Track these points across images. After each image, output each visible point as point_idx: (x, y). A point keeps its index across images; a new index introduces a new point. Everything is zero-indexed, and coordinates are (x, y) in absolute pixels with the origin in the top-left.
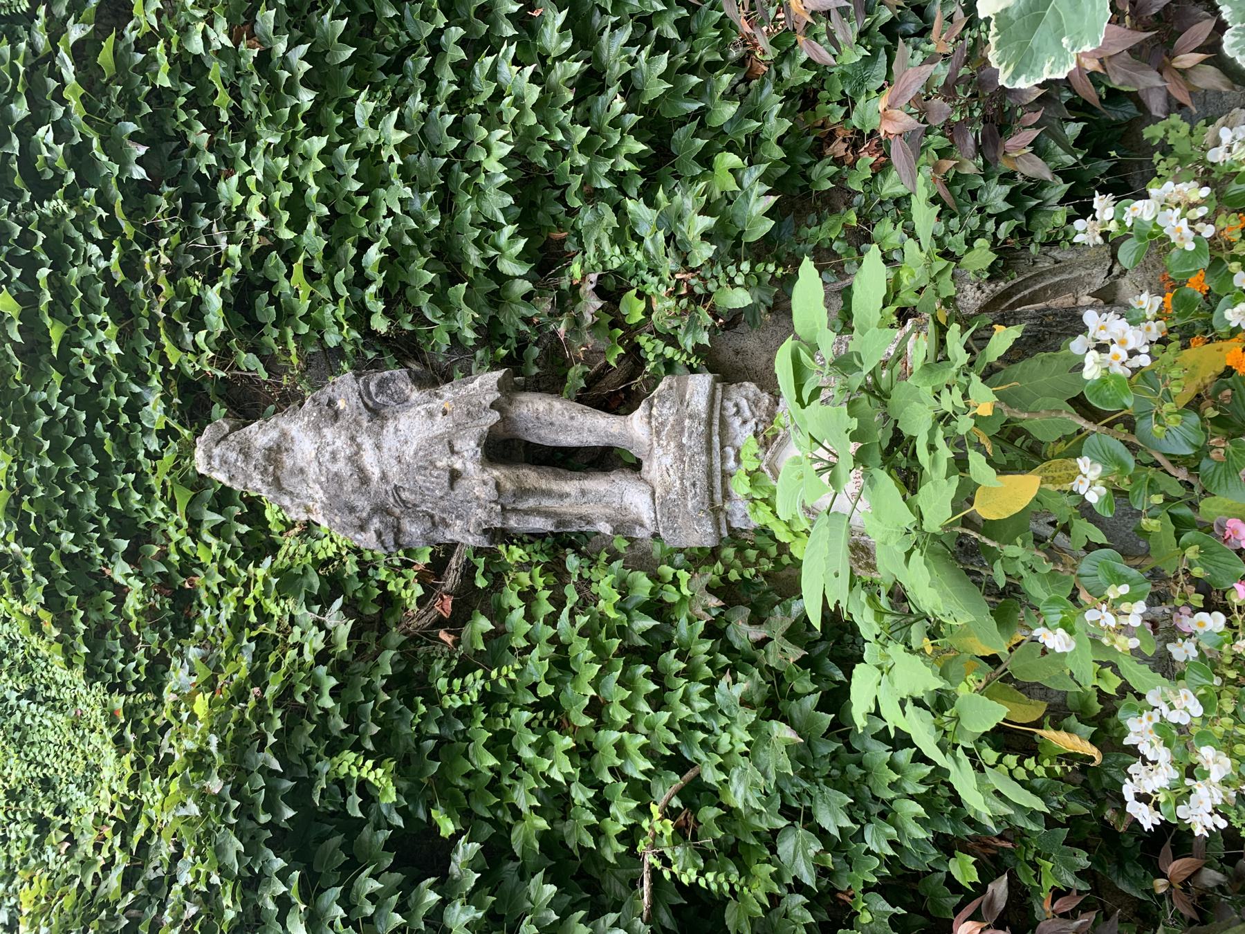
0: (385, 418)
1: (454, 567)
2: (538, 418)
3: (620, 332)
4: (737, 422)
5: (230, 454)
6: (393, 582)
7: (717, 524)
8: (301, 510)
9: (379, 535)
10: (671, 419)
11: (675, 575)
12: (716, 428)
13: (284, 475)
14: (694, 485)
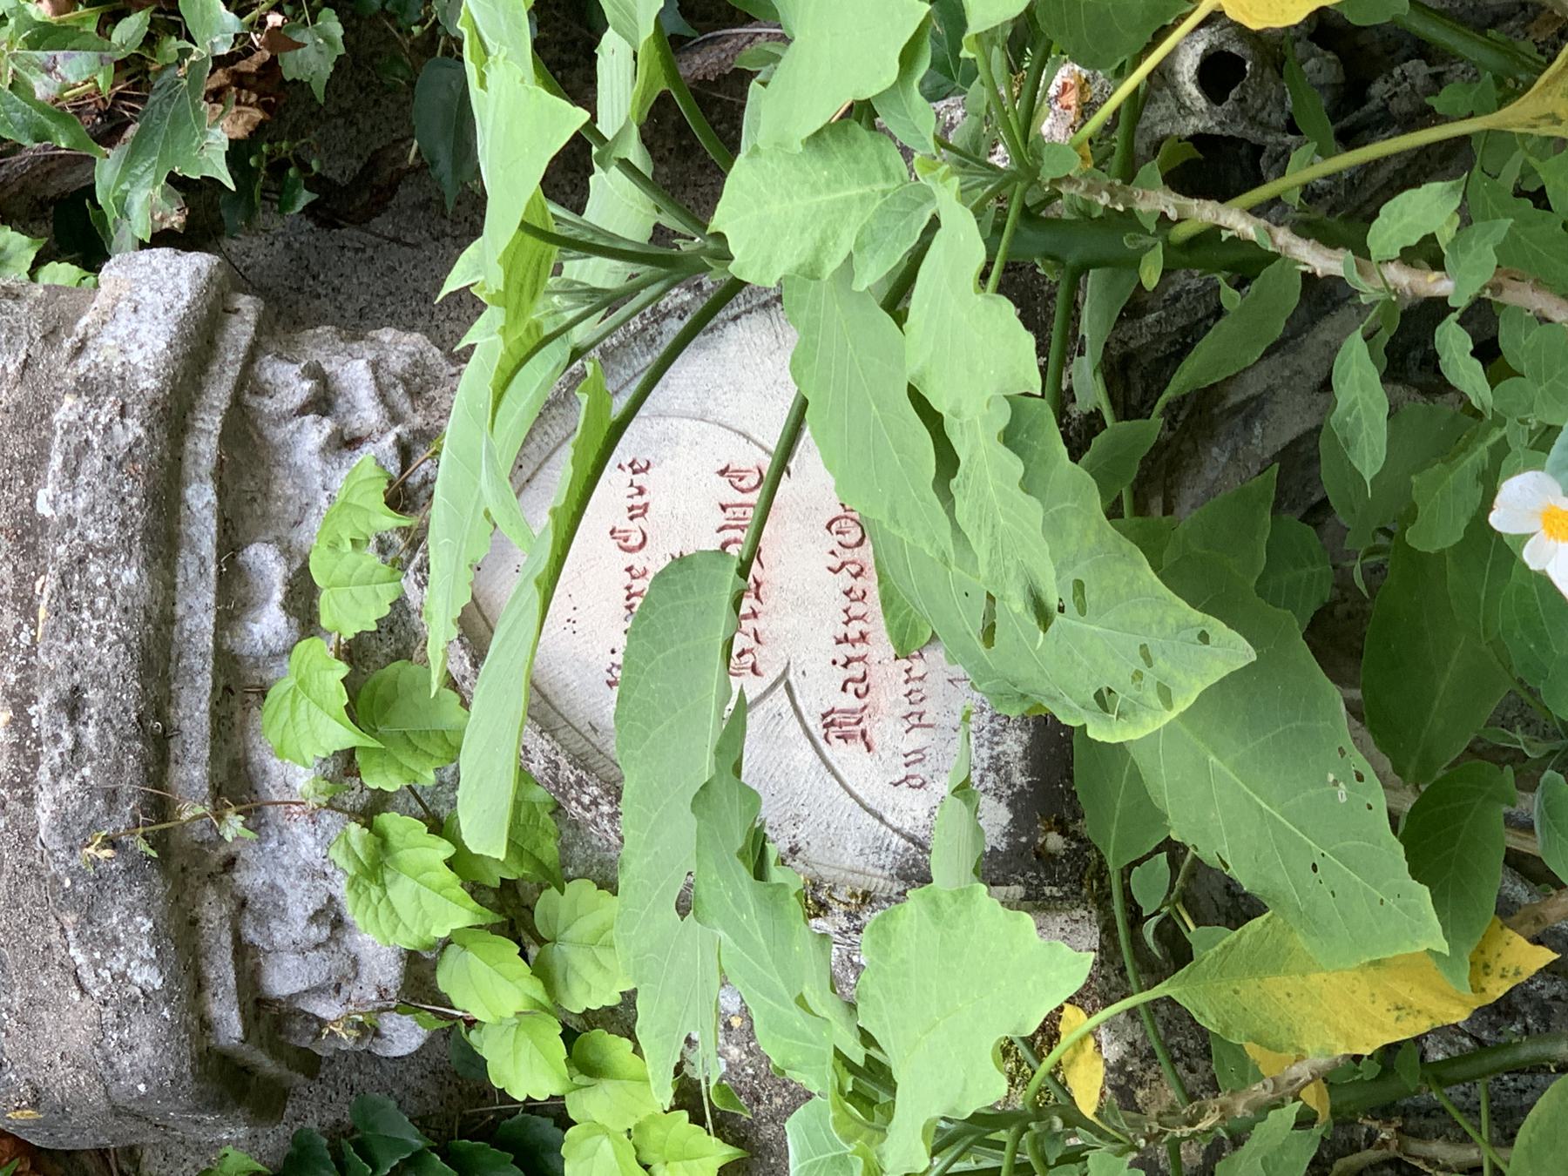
7: (182, 944)
12: (205, 446)
14: (72, 706)
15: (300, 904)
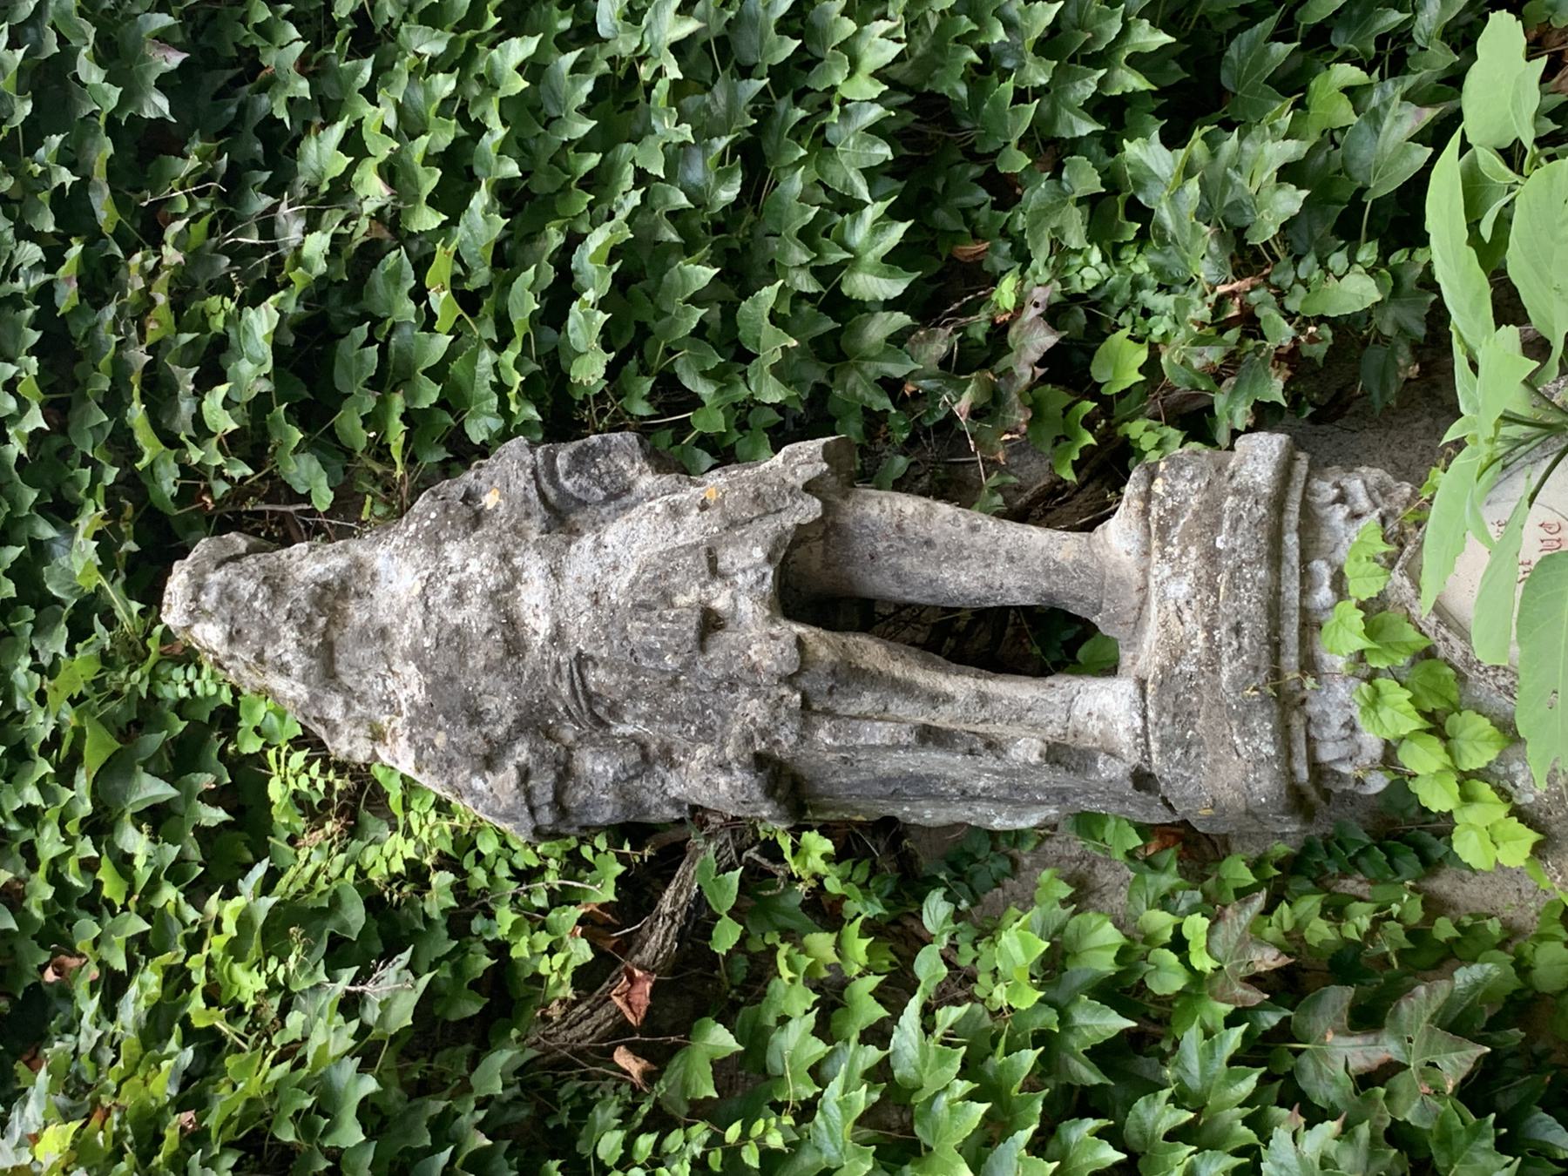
0: (575, 533)
1: (667, 909)
2: (899, 527)
3: (1089, 406)
5: (242, 582)
6: (524, 940)
7: (1284, 736)
8: (361, 731)
9: (525, 774)
10: (1194, 501)
11: (1178, 928)
12: (1293, 517)
13: (345, 638)
14: (1237, 630)
15: (1337, 719)
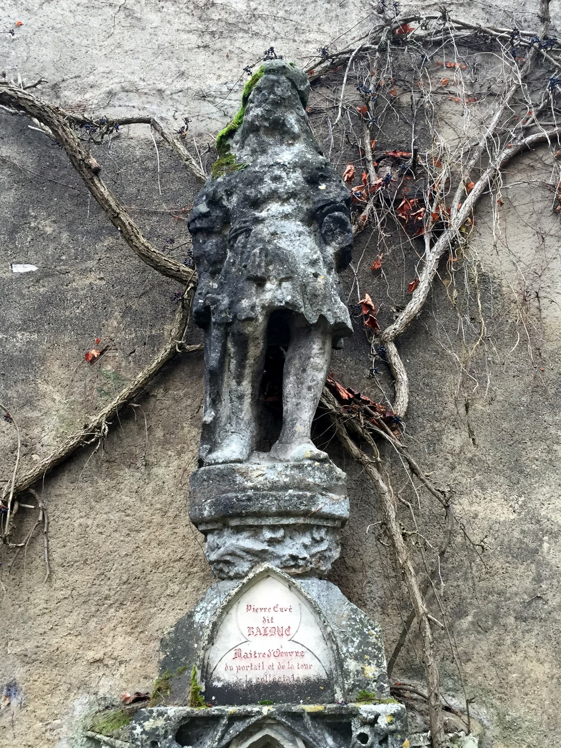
4: (307, 540)
10: (311, 480)
12: (301, 521)
15: (220, 541)
